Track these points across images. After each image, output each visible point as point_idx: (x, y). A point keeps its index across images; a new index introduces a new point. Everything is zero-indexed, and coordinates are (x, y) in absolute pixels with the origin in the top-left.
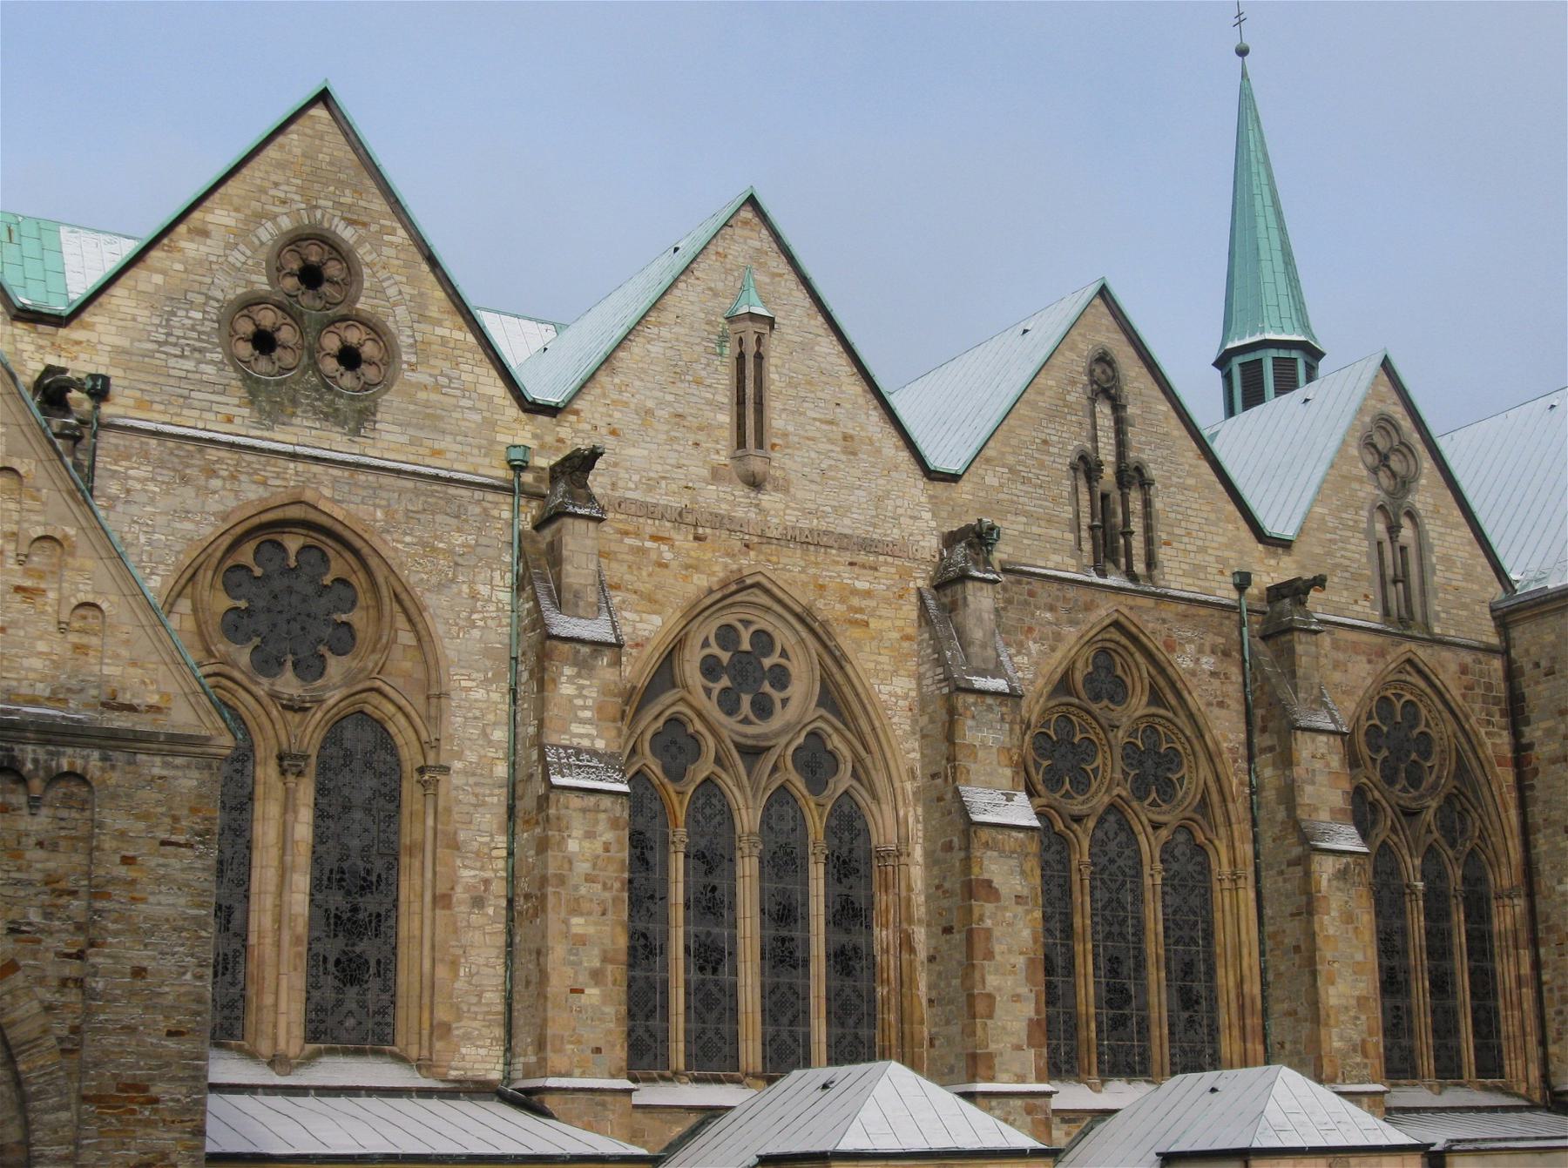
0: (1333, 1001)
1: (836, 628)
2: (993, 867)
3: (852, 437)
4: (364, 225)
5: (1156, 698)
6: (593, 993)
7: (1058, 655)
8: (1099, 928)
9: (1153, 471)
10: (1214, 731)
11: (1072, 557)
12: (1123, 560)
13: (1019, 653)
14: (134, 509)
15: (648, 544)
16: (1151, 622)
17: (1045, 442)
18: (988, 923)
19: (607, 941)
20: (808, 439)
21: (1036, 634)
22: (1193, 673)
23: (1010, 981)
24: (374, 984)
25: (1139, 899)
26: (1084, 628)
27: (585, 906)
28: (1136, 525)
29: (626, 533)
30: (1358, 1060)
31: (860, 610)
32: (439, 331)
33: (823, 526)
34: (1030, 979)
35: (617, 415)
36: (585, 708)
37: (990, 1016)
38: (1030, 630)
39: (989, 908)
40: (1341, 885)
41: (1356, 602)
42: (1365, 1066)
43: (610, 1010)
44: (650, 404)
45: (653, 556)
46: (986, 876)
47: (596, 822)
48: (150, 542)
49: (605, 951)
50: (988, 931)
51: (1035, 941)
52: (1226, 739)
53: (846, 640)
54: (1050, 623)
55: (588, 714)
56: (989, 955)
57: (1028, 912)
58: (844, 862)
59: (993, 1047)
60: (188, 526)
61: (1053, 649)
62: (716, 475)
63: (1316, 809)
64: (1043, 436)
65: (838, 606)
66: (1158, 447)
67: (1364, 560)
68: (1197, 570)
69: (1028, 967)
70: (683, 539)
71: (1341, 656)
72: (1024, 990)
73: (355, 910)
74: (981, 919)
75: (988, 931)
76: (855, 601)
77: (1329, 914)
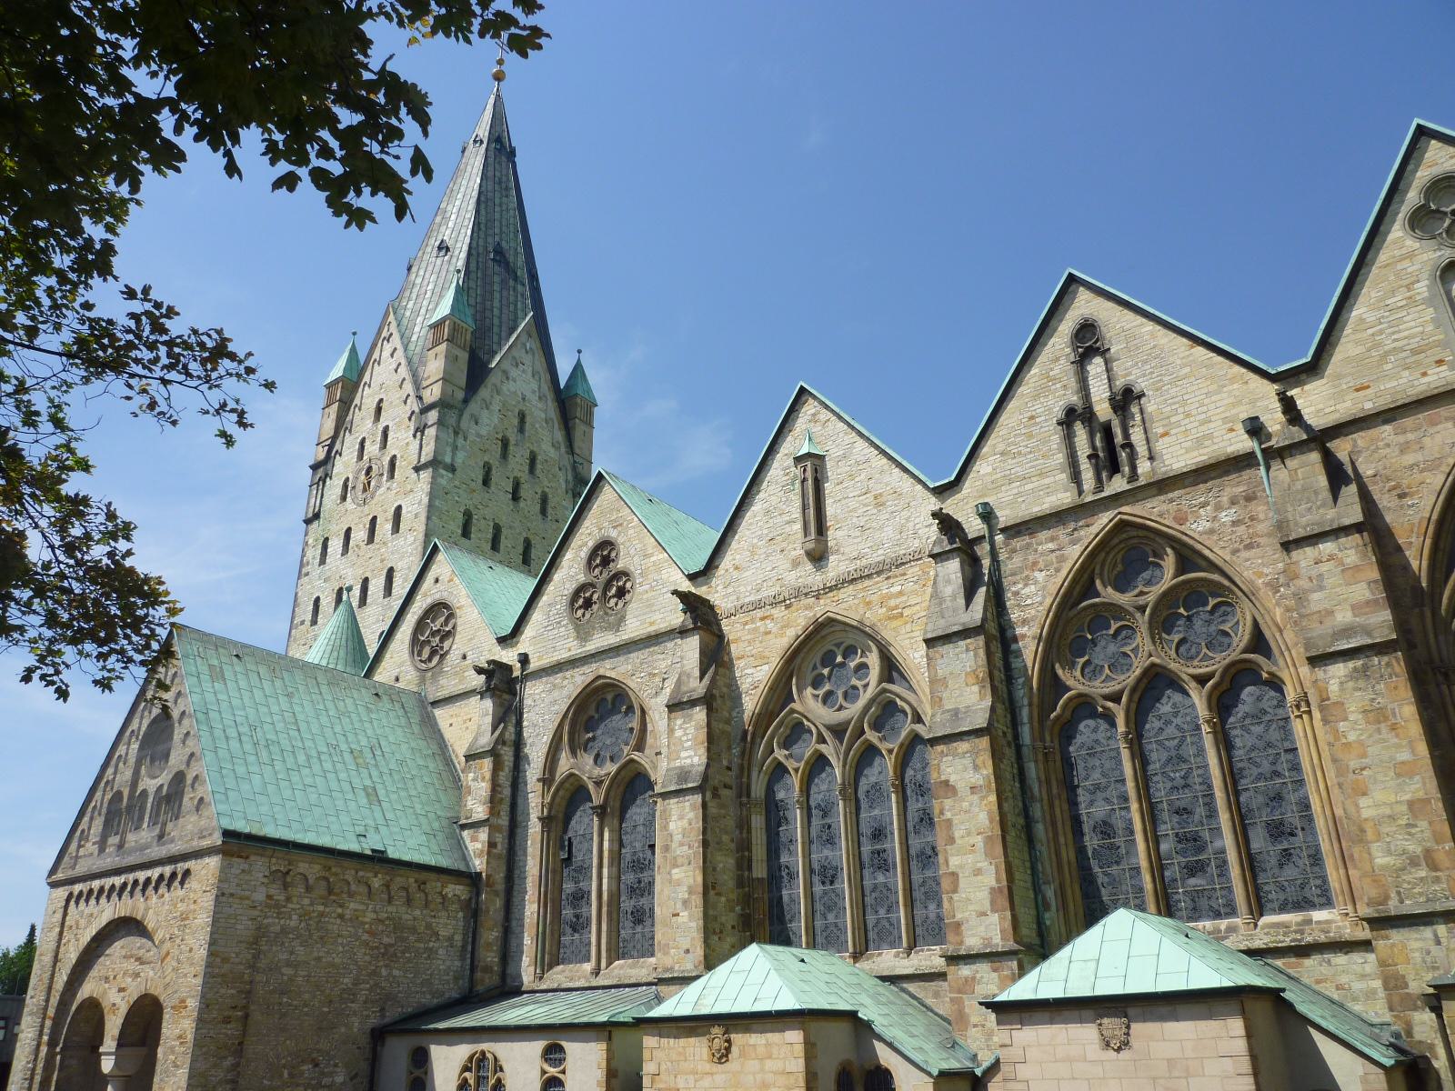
0: (1366, 813)
1: (879, 627)
2: (949, 770)
3: (881, 495)
4: (621, 525)
5: (1181, 569)
6: (684, 914)
7: (1064, 572)
8: (1198, 780)
9: (1141, 385)
10: (1245, 574)
11: (1066, 491)
12: (1127, 469)
13: (1026, 585)
14: (537, 708)
15: (758, 624)
16: (1154, 511)
17: (1032, 418)
18: (948, 815)
19: (691, 881)
20: (851, 511)
21: (1041, 565)
22: (1212, 531)
23: (970, 859)
24: (648, 922)
25: (1201, 752)
26: (1086, 542)
27: (680, 861)
28: (1137, 436)
29: (746, 624)
30: (1423, 874)
31: (896, 607)
32: (653, 559)
33: (864, 562)
34: (988, 854)
35: (738, 557)
36: (688, 740)
37: (955, 891)
38: (1035, 564)
39: (948, 803)
40: (1361, 683)
41: (1424, 374)
42: (1437, 880)
43: (693, 924)
44: (755, 541)
45: (762, 629)
46: (943, 778)
47: (684, 807)
48: (543, 721)
49: (690, 887)
50: (949, 822)
51: (991, 822)
52: (1261, 575)
53: (887, 634)
54: (1053, 551)
55: (690, 743)
56: (951, 840)
57: (982, 798)
58: (920, 786)
59: (959, 916)
60: (557, 707)
61: (1058, 570)
62: (796, 564)
63: (1330, 613)
64: (1029, 414)
65: (880, 611)
66: (1145, 362)
67: (1430, 328)
68: (1199, 443)
69: (986, 843)
70: (778, 612)
71: (1410, 436)
72: (984, 865)
73: (640, 882)
74: (942, 813)
75: (949, 822)
76: (892, 603)
77: (1346, 719)
